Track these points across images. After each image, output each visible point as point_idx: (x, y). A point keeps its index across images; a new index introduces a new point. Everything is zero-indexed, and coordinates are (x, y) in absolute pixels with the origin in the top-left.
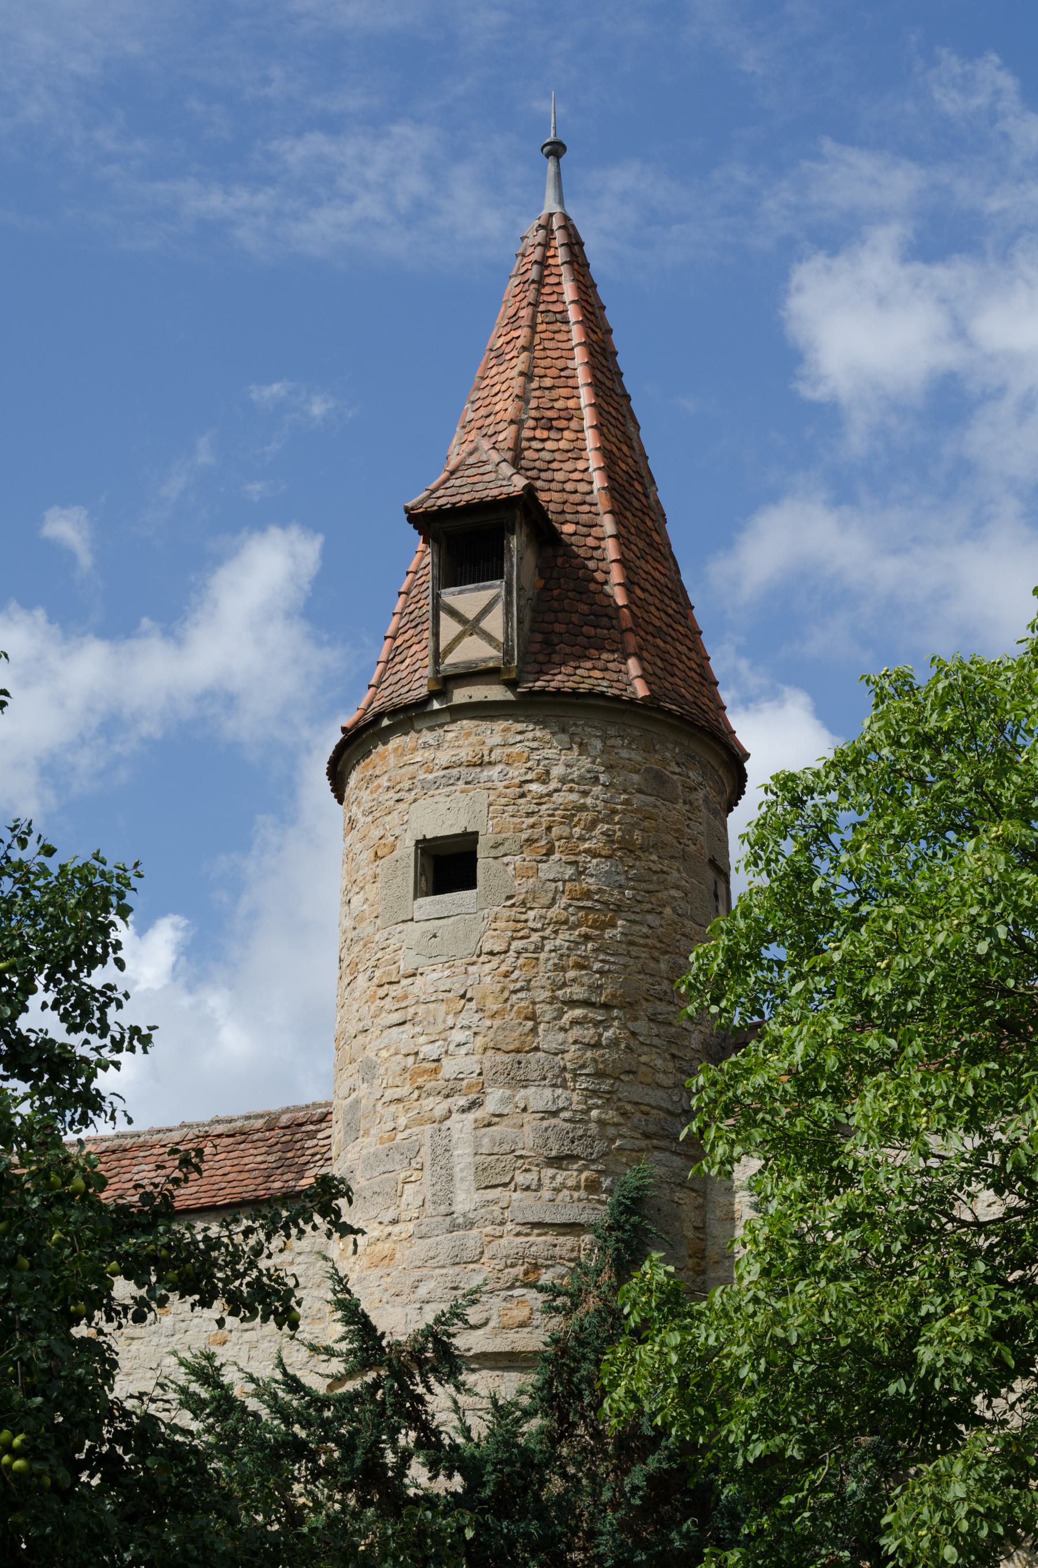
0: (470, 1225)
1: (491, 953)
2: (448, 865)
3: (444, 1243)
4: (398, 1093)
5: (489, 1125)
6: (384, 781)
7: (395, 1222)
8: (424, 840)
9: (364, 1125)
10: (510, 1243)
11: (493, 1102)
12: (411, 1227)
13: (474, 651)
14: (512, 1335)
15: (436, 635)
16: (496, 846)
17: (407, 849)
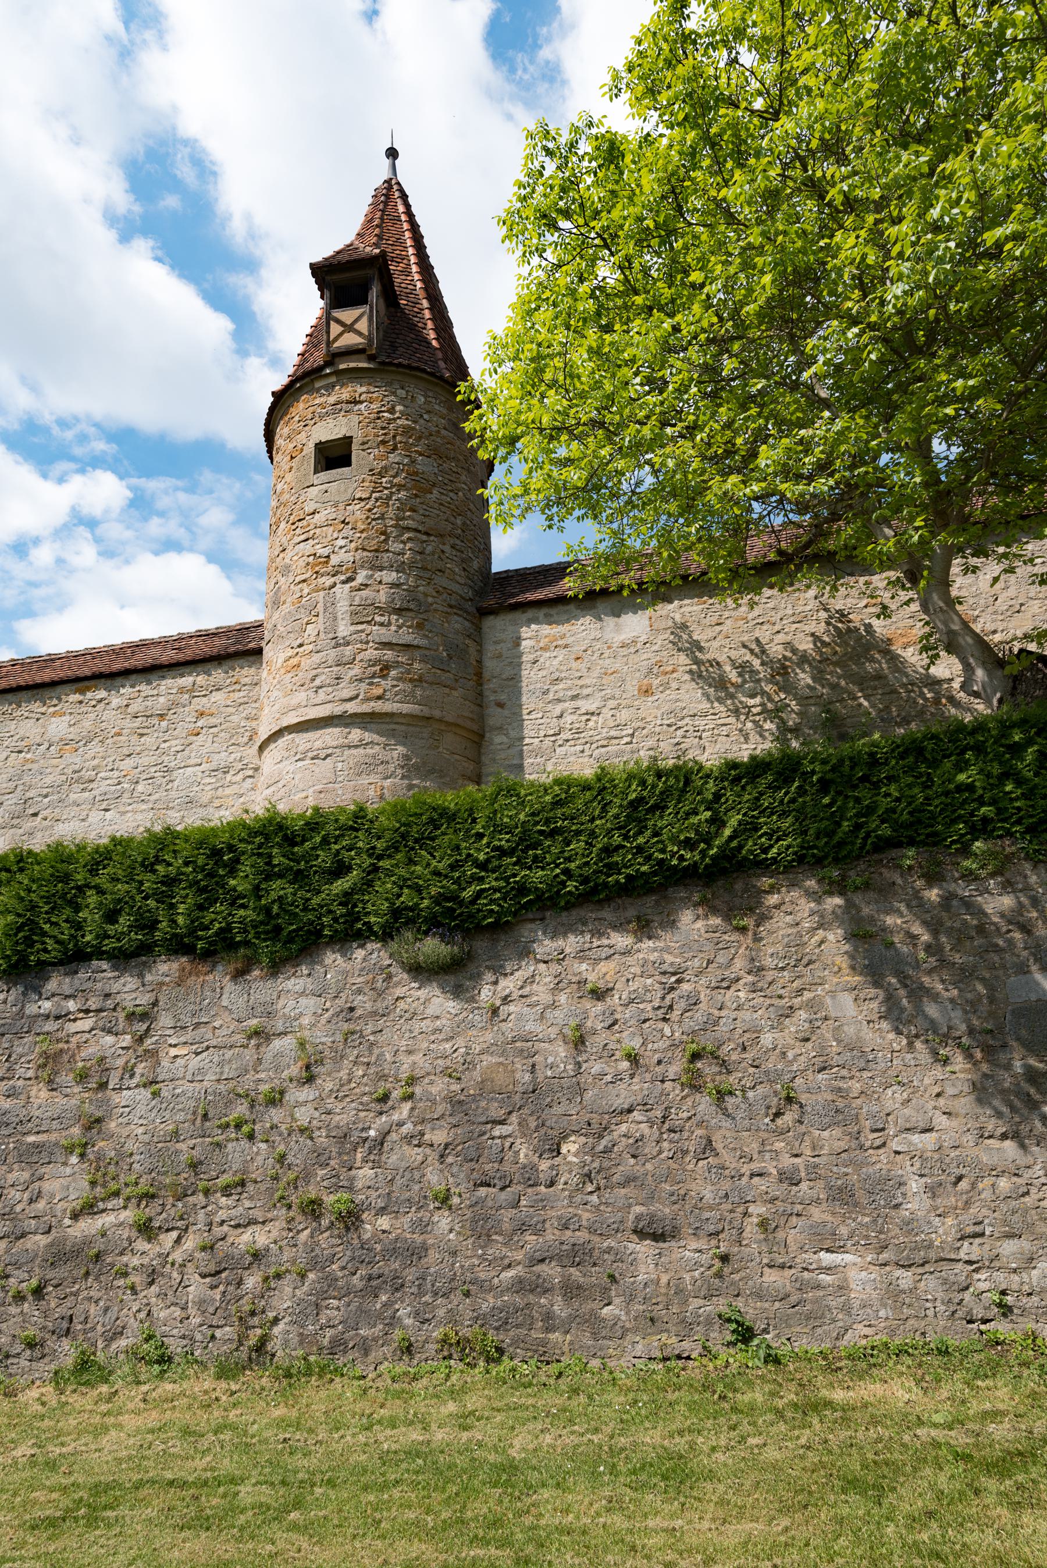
0: (348, 644)
1: (360, 499)
2: (333, 456)
3: (332, 654)
4: (303, 577)
5: (359, 590)
6: (297, 418)
7: (301, 645)
8: (321, 443)
9: (283, 599)
10: (371, 653)
11: (361, 578)
12: (311, 647)
13: (350, 340)
14: (372, 704)
15: (328, 332)
16: (363, 443)
17: (310, 449)
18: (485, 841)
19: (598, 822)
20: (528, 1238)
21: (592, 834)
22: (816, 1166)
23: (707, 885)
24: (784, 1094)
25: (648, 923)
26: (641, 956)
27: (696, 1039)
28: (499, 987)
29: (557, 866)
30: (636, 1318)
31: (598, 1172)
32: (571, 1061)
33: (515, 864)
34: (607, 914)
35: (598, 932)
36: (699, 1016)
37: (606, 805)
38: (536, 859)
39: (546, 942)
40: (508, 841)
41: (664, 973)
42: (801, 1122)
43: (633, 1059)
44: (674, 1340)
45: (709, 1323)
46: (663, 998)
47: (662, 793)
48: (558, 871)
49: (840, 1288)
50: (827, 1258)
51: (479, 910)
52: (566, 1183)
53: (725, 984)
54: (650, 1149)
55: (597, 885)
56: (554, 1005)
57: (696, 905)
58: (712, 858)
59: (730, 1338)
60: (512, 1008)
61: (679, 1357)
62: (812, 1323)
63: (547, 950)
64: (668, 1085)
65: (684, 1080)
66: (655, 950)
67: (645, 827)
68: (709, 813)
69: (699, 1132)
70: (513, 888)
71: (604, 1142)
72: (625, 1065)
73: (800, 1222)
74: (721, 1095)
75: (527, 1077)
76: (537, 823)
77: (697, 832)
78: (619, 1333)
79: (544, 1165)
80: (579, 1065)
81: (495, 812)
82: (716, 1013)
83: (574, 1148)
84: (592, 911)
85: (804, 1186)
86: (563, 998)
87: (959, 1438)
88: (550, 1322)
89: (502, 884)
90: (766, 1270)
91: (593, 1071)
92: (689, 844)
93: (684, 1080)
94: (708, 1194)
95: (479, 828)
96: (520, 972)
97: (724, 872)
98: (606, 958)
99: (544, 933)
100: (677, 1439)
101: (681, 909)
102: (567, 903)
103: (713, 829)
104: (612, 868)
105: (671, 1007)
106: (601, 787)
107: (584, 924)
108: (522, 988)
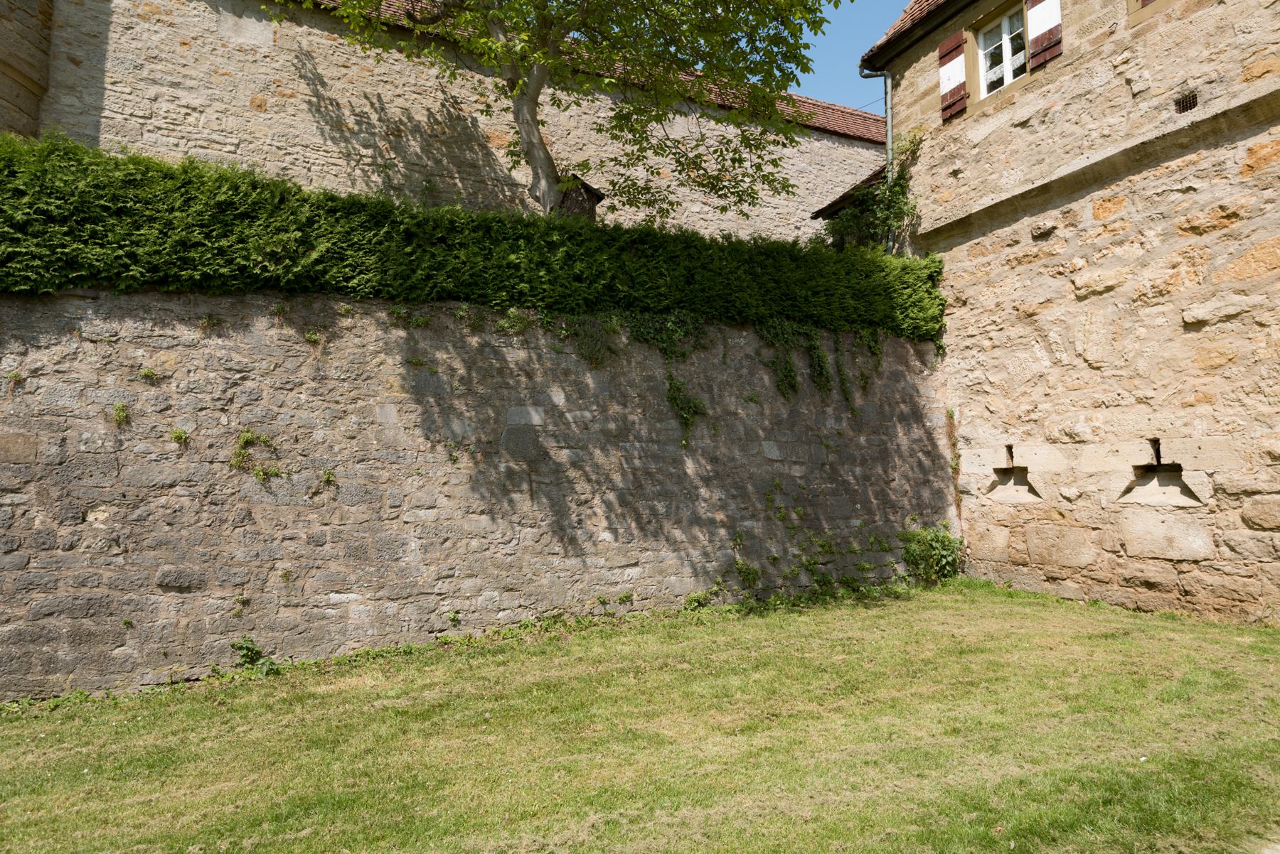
18: (26, 199)
19: (177, 214)
20: (34, 596)
21: (169, 224)
22: (340, 532)
23: (286, 299)
24: (325, 478)
25: (220, 323)
26: (207, 351)
27: (252, 430)
28: (28, 359)
29: (121, 247)
30: (148, 655)
31: (128, 537)
32: (111, 438)
33: (65, 234)
34: (175, 306)
35: (163, 322)
36: (258, 411)
37: (190, 199)
38: (94, 234)
39: (97, 322)
40: (58, 207)
41: (230, 370)
42: (335, 500)
43: (184, 442)
44: (185, 667)
45: (222, 651)
46: (225, 391)
47: (254, 203)
48: (121, 252)
49: (341, 617)
50: (334, 597)
51: (8, 274)
52: (88, 547)
53: (288, 386)
54: (188, 518)
55: (166, 276)
56: (97, 385)
57: (273, 314)
58: (295, 274)
59: (238, 660)
60: (43, 381)
61: (188, 680)
62: (313, 643)
63: (98, 330)
64: (216, 466)
65: (233, 462)
66: (223, 347)
67: (231, 232)
68: (300, 234)
69: (240, 505)
70: (59, 259)
71: (138, 512)
72: (174, 446)
73: (319, 573)
74: (267, 476)
75: (54, 450)
76: (101, 197)
77: (284, 249)
78: (129, 668)
79: (64, 531)
80: (121, 443)
81: (45, 172)
82: (276, 409)
83: (102, 516)
84: (158, 301)
85: (327, 547)
86: (110, 379)
87: (403, 703)
88: (50, 665)
89: (45, 251)
90: (282, 609)
91: (136, 449)
92: (273, 257)
93: (233, 462)
94: (240, 554)
95: (19, 183)
96: (58, 347)
97: (305, 290)
98: (168, 348)
99: (96, 313)
100: (170, 738)
101: (257, 316)
102: (128, 287)
103: (301, 250)
104: (186, 263)
105: (231, 400)
106: (187, 180)
107: (148, 311)
108: (59, 363)
